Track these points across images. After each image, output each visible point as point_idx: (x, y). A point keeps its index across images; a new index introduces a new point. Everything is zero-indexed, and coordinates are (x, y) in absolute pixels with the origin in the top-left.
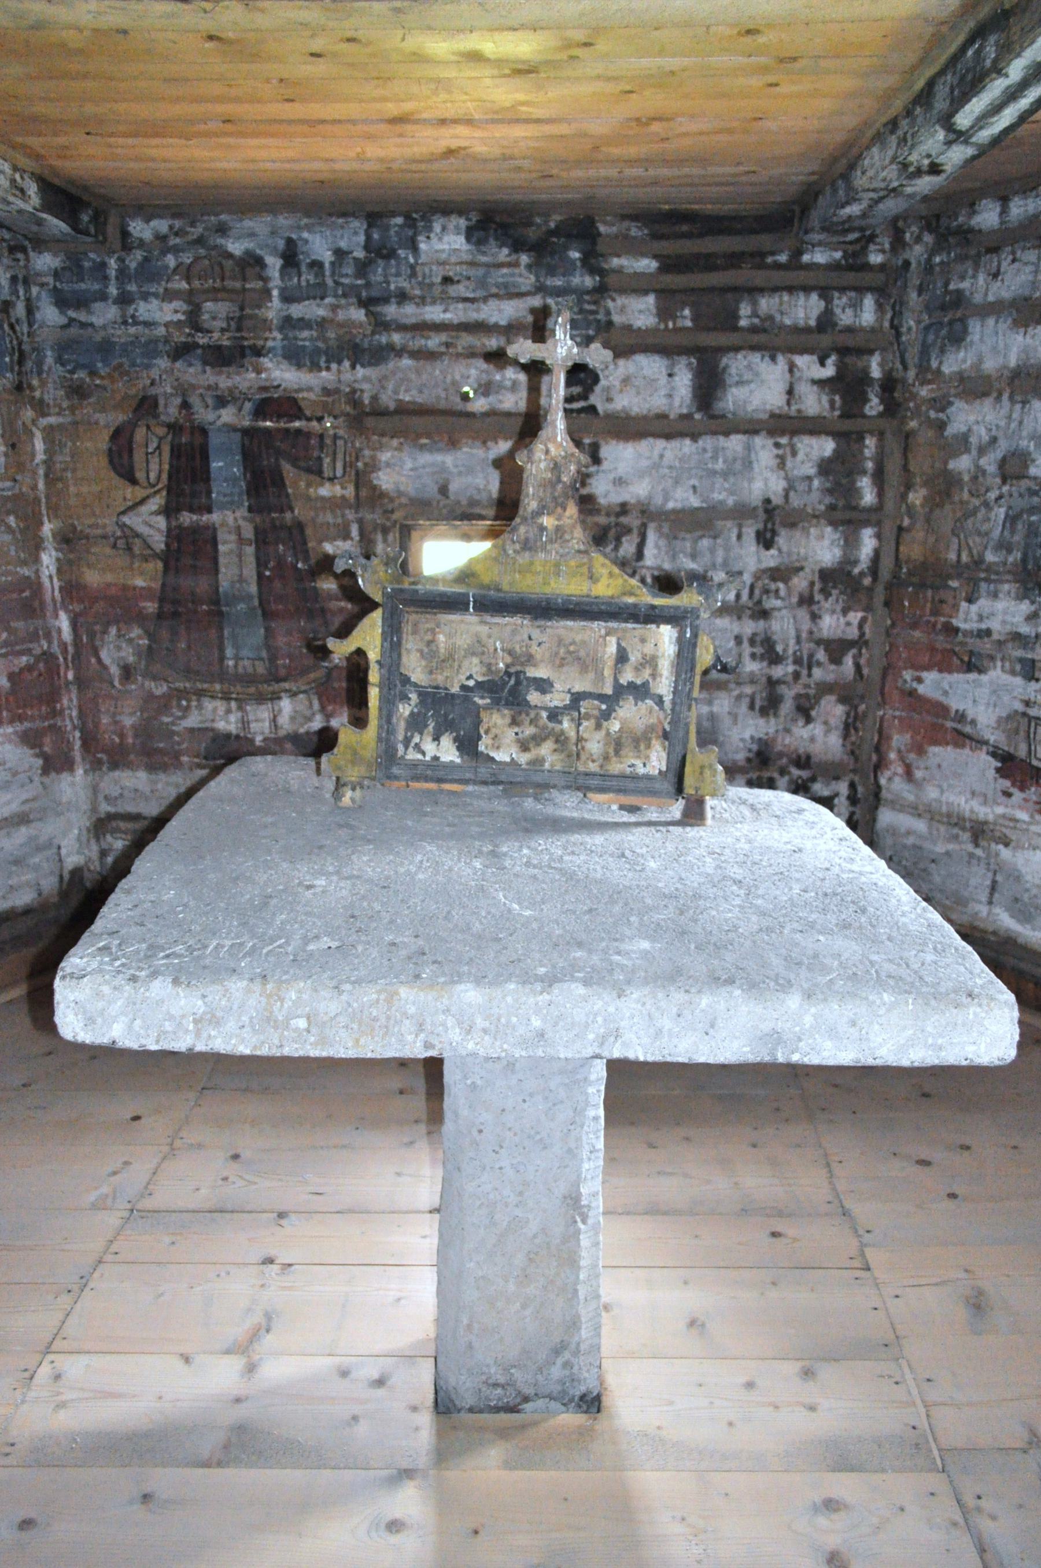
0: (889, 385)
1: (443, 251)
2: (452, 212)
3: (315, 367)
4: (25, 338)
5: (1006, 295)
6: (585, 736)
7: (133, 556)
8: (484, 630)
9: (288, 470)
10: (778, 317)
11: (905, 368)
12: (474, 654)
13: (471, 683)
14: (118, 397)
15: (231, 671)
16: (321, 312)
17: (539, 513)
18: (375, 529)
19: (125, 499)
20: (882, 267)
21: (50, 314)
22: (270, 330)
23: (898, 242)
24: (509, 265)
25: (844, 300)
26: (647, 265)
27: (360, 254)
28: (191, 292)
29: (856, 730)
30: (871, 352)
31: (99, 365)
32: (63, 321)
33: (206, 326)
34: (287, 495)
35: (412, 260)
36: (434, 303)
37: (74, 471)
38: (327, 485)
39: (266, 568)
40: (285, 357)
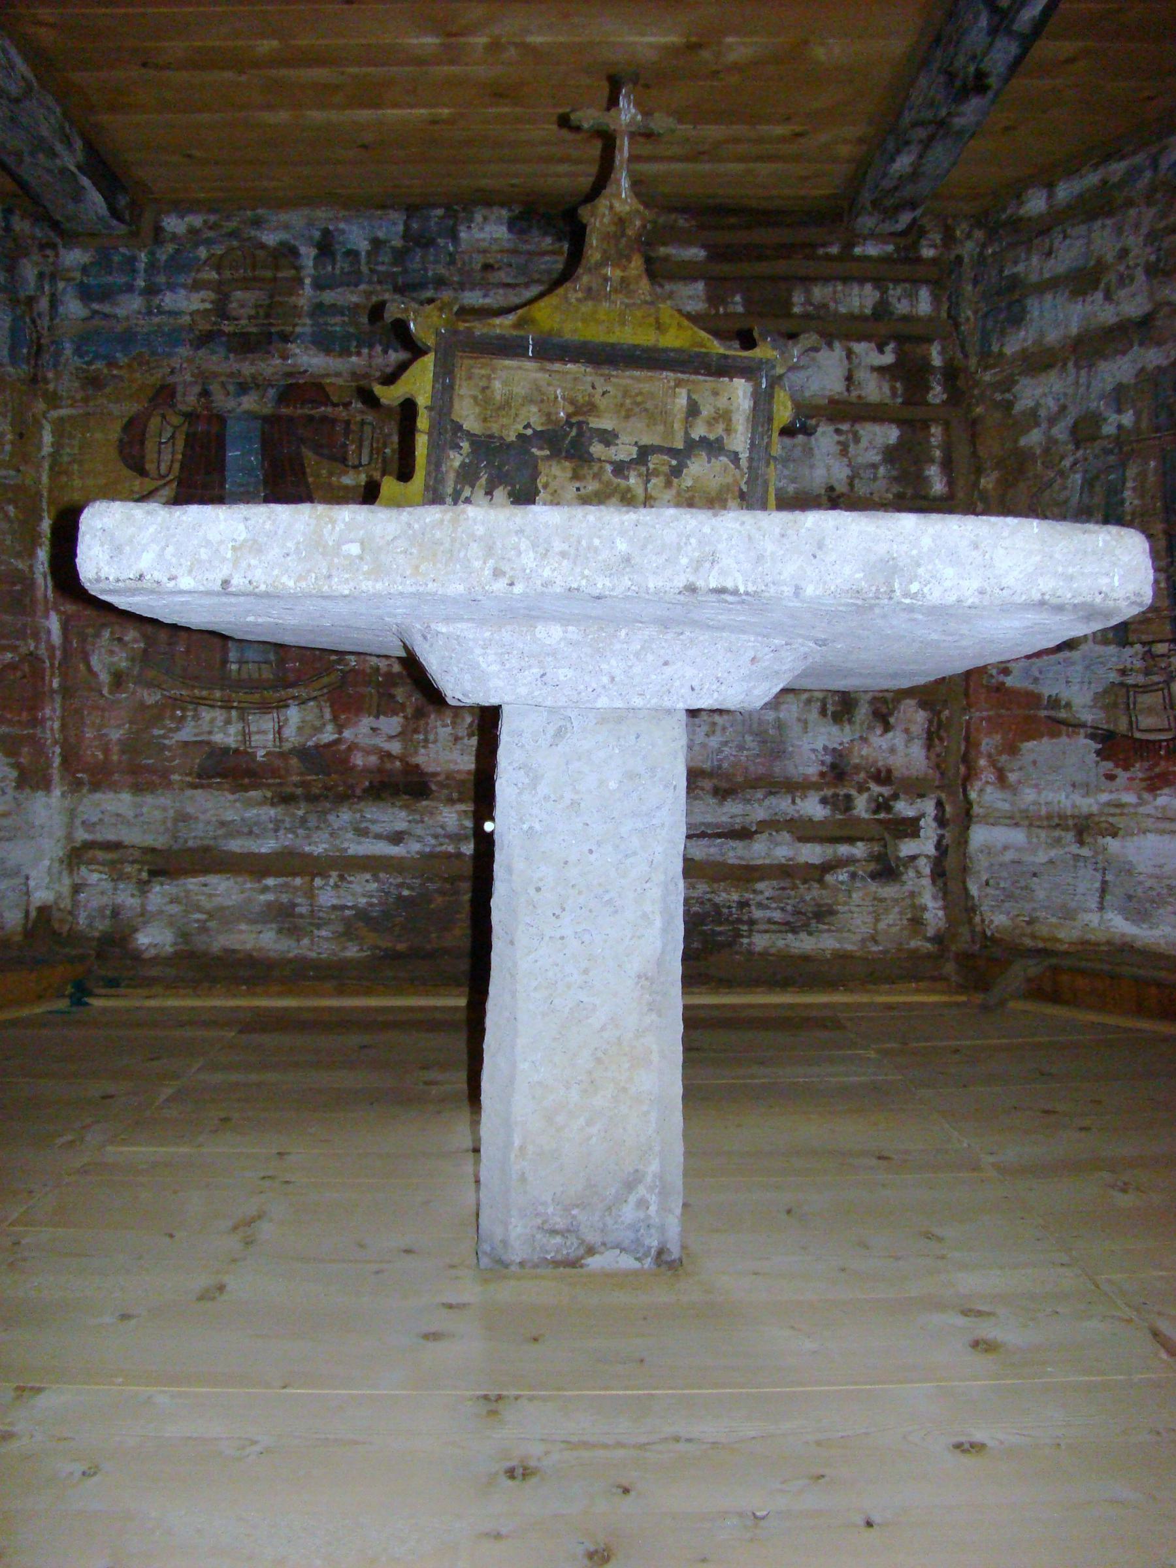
0: (951, 374)
1: (484, 240)
2: (495, 204)
3: (345, 352)
4: (45, 333)
5: (1060, 269)
6: (654, 494)
8: (542, 377)
9: (309, 456)
10: (832, 305)
11: (966, 356)
12: (532, 401)
13: (529, 432)
15: (234, 675)
16: (354, 299)
17: (603, 263)
20: (934, 261)
21: (73, 308)
23: (949, 239)
24: (553, 253)
25: (899, 291)
26: (696, 253)
27: (397, 243)
28: (220, 283)
29: (941, 739)
30: (929, 341)
31: (118, 355)
33: (234, 313)
35: (451, 249)
36: (472, 289)
37: (81, 463)
38: (351, 472)
40: (313, 343)
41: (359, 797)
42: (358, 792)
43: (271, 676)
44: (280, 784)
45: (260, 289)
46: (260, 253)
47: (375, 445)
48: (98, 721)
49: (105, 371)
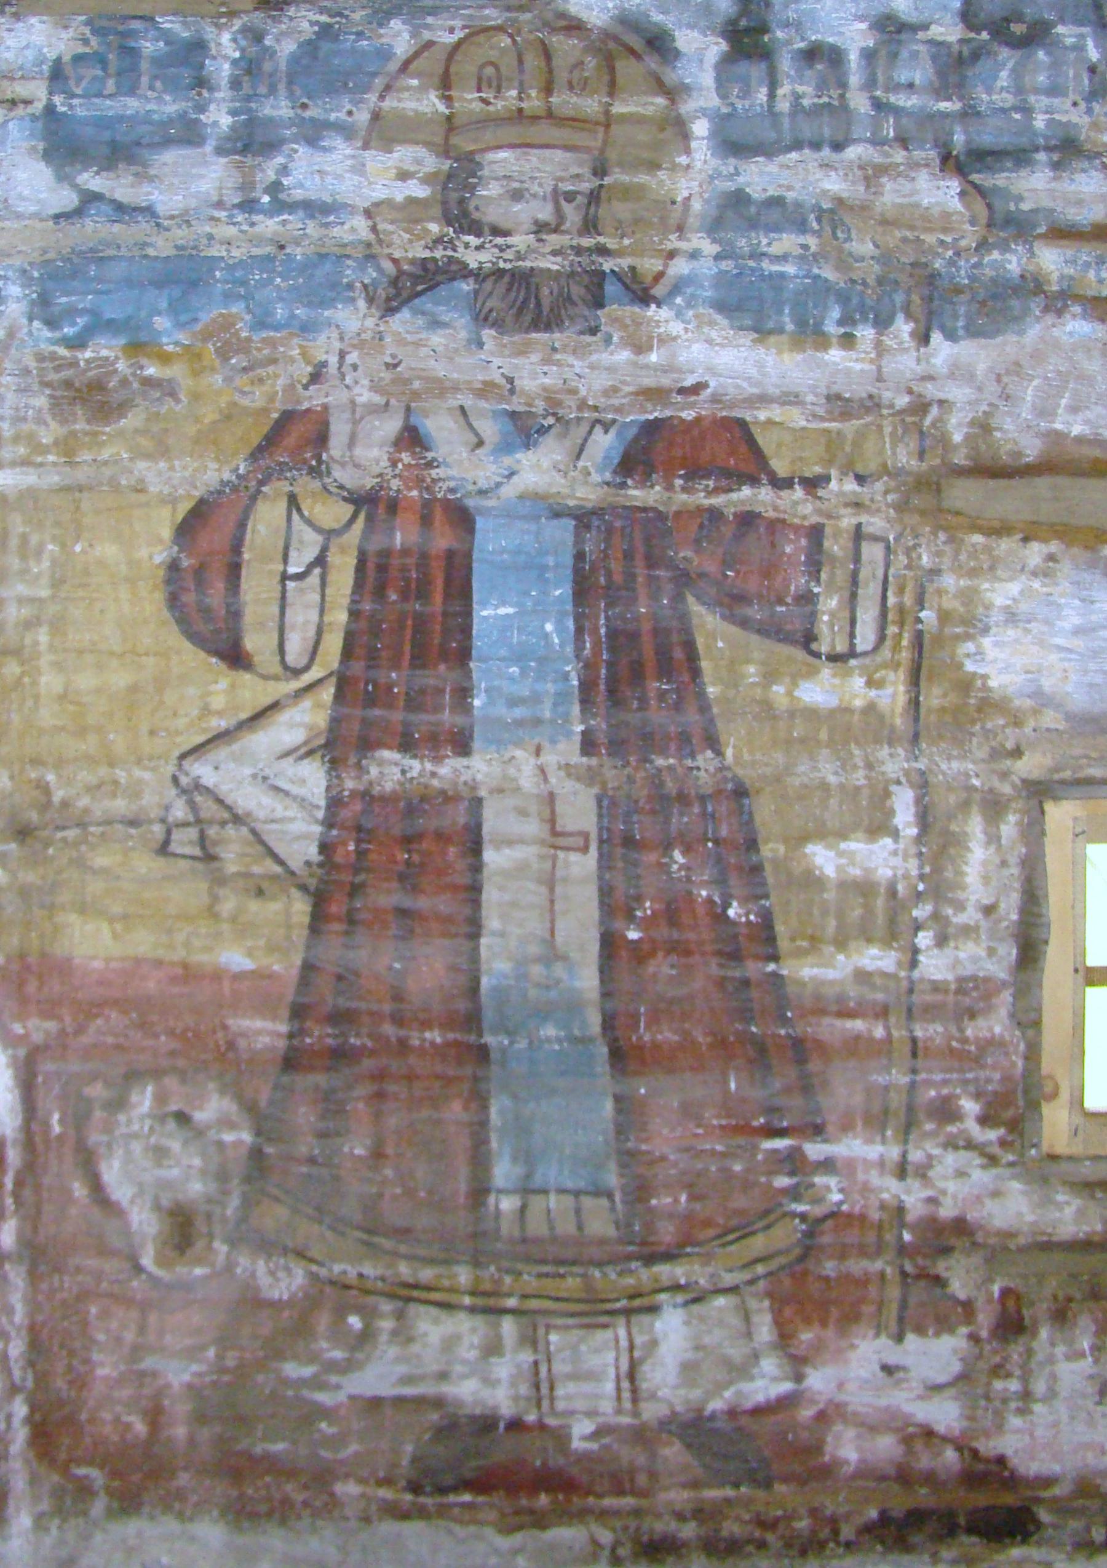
7: (220, 880)
14: (210, 415)
15: (508, 1228)
16: (834, 184)
18: (965, 806)
19: (206, 711)
22: (680, 229)
31: (161, 322)
32: (68, 199)
33: (492, 215)
34: (704, 707)
37: (58, 626)
38: (826, 672)
39: (630, 917)
40: (721, 307)
41: (848, 1545)
42: (847, 1532)
43: (611, 1232)
44: (637, 1513)
45: (567, 148)
46: (566, 47)
47: (891, 600)
48: (129, 1336)
49: (121, 366)
